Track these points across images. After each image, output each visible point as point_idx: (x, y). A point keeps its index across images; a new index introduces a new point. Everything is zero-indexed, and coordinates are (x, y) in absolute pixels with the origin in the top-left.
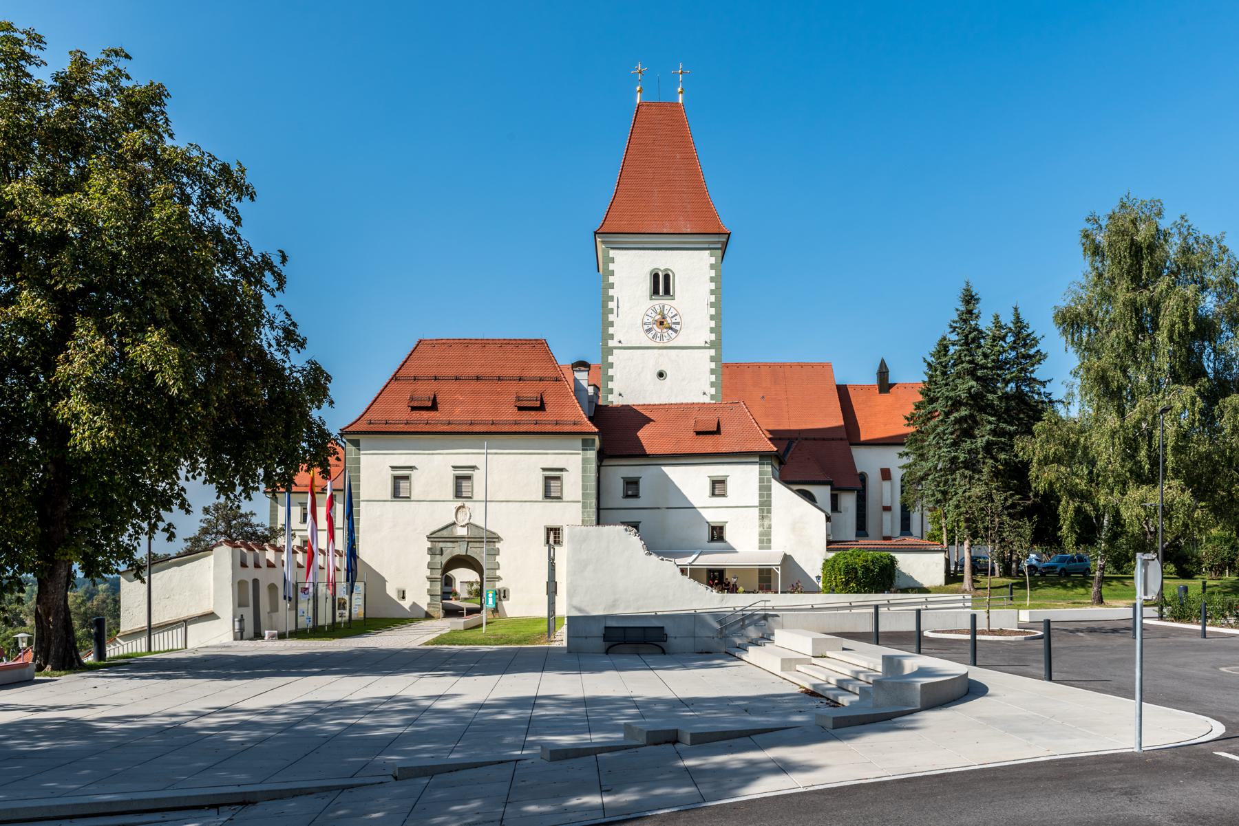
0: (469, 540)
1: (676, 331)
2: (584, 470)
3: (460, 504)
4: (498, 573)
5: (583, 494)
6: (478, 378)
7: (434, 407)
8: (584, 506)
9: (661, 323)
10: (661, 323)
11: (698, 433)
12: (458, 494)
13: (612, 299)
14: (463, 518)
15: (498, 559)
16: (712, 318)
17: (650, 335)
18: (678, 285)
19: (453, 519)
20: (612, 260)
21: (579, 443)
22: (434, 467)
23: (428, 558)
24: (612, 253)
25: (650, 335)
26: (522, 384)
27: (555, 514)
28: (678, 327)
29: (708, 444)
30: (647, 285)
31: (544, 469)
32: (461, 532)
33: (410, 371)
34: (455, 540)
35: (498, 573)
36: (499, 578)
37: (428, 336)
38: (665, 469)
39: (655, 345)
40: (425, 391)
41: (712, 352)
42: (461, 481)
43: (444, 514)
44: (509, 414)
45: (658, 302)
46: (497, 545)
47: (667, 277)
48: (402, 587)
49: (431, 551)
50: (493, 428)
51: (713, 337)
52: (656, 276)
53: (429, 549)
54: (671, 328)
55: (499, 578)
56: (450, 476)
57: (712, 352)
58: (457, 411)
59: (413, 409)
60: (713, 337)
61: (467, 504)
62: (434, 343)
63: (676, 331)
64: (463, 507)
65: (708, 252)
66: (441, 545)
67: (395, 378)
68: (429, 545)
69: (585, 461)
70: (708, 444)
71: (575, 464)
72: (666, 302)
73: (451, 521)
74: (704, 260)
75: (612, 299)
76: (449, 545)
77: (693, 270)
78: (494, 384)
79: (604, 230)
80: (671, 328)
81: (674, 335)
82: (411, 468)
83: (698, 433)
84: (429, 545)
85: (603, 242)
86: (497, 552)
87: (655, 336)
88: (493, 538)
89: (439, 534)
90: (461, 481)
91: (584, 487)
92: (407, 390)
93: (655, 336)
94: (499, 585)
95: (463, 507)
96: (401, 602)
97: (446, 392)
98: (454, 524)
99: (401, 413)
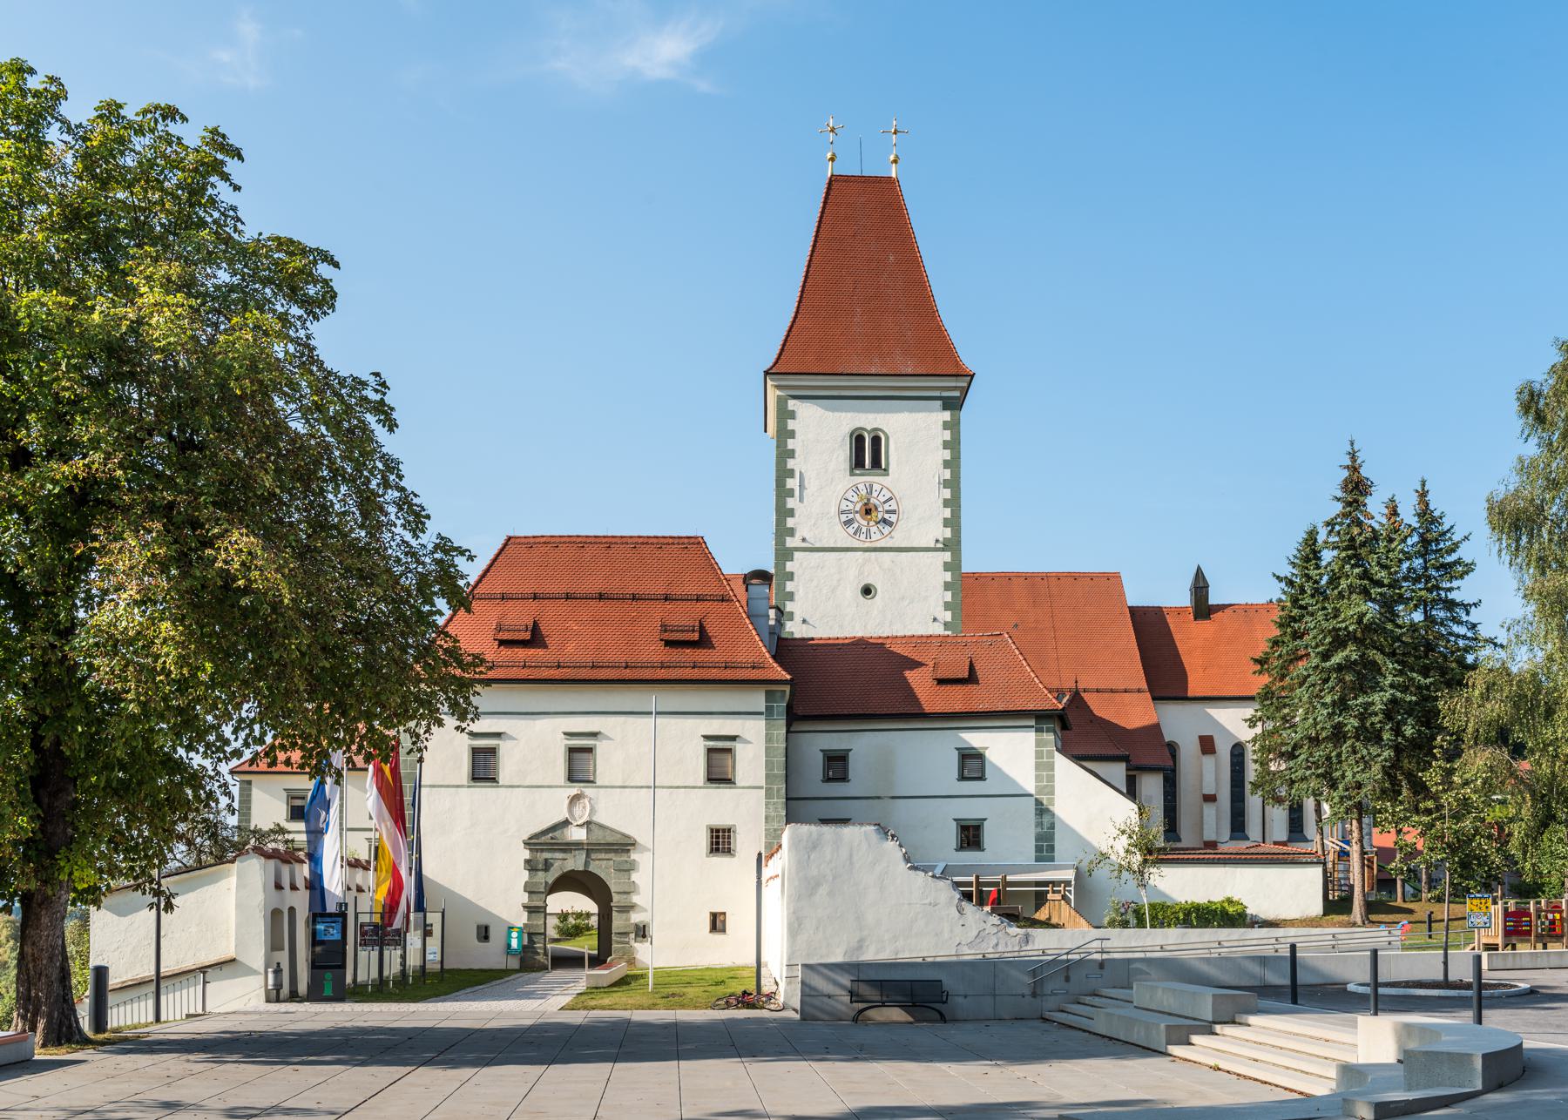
0: (590, 849)
1: (890, 524)
3: (574, 791)
4: (635, 899)
5: (767, 776)
6: (601, 597)
8: (769, 795)
11: (941, 682)
12: (572, 778)
13: (791, 473)
15: (635, 877)
17: (851, 530)
18: (894, 454)
20: (792, 415)
22: (533, 738)
23: (525, 876)
25: (851, 530)
26: (669, 606)
27: (722, 806)
28: (893, 518)
30: (844, 454)
32: (577, 834)
39: (857, 544)
43: (551, 807)
44: (653, 651)
45: (862, 480)
47: (876, 441)
49: (530, 865)
50: (628, 674)
52: (859, 440)
53: (527, 862)
58: (571, 647)
59: (502, 643)
61: (589, 791)
63: (890, 524)
68: (527, 854)
72: (877, 480)
75: (791, 473)
76: (558, 855)
78: (626, 606)
83: (941, 682)
84: (527, 854)
88: (623, 846)
89: (543, 839)
91: (769, 765)
94: (635, 918)
98: (566, 823)
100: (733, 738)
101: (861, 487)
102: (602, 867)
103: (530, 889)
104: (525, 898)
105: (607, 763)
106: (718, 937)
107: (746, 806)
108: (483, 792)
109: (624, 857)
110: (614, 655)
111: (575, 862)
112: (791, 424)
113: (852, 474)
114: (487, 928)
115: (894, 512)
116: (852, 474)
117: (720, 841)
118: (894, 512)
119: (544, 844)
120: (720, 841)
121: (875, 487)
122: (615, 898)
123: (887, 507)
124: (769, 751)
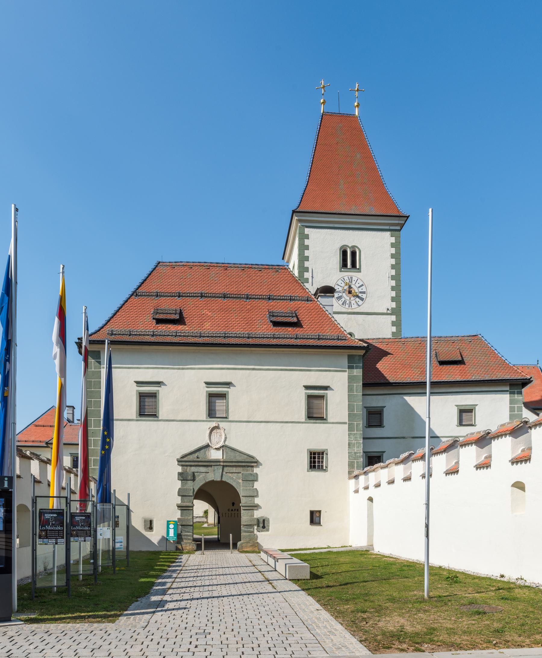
0: (225, 464)
1: (362, 299)
2: (350, 389)
3: (214, 424)
4: (257, 501)
5: (350, 415)
6: (225, 296)
7: (180, 321)
8: (351, 429)
9: (350, 292)
10: (350, 292)
11: (442, 363)
12: (211, 413)
13: (307, 270)
14: (218, 440)
15: (256, 485)
16: (393, 288)
18: (364, 260)
19: (206, 441)
20: (307, 237)
21: (345, 361)
22: (184, 383)
23: (178, 484)
24: (307, 231)
26: (272, 303)
27: (317, 436)
28: (364, 296)
29: (452, 374)
30: (337, 259)
31: (307, 387)
33: (153, 287)
34: (210, 464)
35: (257, 501)
36: (257, 507)
37: (167, 258)
38: (408, 398)
39: (344, 310)
40: (169, 305)
41: (393, 318)
42: (216, 399)
43: (196, 435)
44: (264, 329)
45: (346, 275)
46: (256, 470)
47: (354, 254)
48: (149, 516)
49: (182, 477)
50: (250, 341)
51: (394, 305)
52: (344, 253)
53: (180, 474)
54: (358, 296)
55: (257, 507)
56: (202, 392)
57: (393, 318)
58: (207, 325)
59: (159, 321)
60: (394, 305)
61: (222, 425)
62: (173, 266)
63: (362, 299)
64: (217, 427)
65: (388, 233)
66: (193, 469)
67: (135, 293)
68: (180, 469)
69: (351, 379)
70: (452, 374)
71: (340, 383)
72: (354, 275)
73: (204, 443)
74: (385, 239)
75: (307, 270)
76: (202, 469)
77: (375, 247)
78: (243, 302)
79: (297, 210)
80: (358, 296)
81: (360, 302)
82: (159, 383)
83: (442, 363)
84: (180, 469)
85: (299, 221)
86: (255, 478)
87: (344, 303)
88: (248, 463)
89: (191, 458)
90: (216, 399)
91: (351, 408)
92: (150, 304)
93: (344, 303)
94: (257, 514)
95: (217, 427)
96: (148, 534)
97: (190, 308)
98: (208, 446)
99: (145, 325)
100: (326, 388)
101: (346, 278)
102: (234, 478)
103: (182, 493)
104: (179, 500)
105: (238, 403)
106: (316, 528)
107: (337, 436)
108: (147, 425)
109: (249, 471)
110: (239, 330)
111: (214, 475)
112: (307, 242)
113: (341, 271)
114: (151, 522)
115: (364, 293)
116: (341, 271)
117: (316, 460)
118: (364, 293)
119: (192, 461)
120: (316, 460)
121: (354, 279)
122: (243, 501)
123: (360, 290)
124: (351, 398)
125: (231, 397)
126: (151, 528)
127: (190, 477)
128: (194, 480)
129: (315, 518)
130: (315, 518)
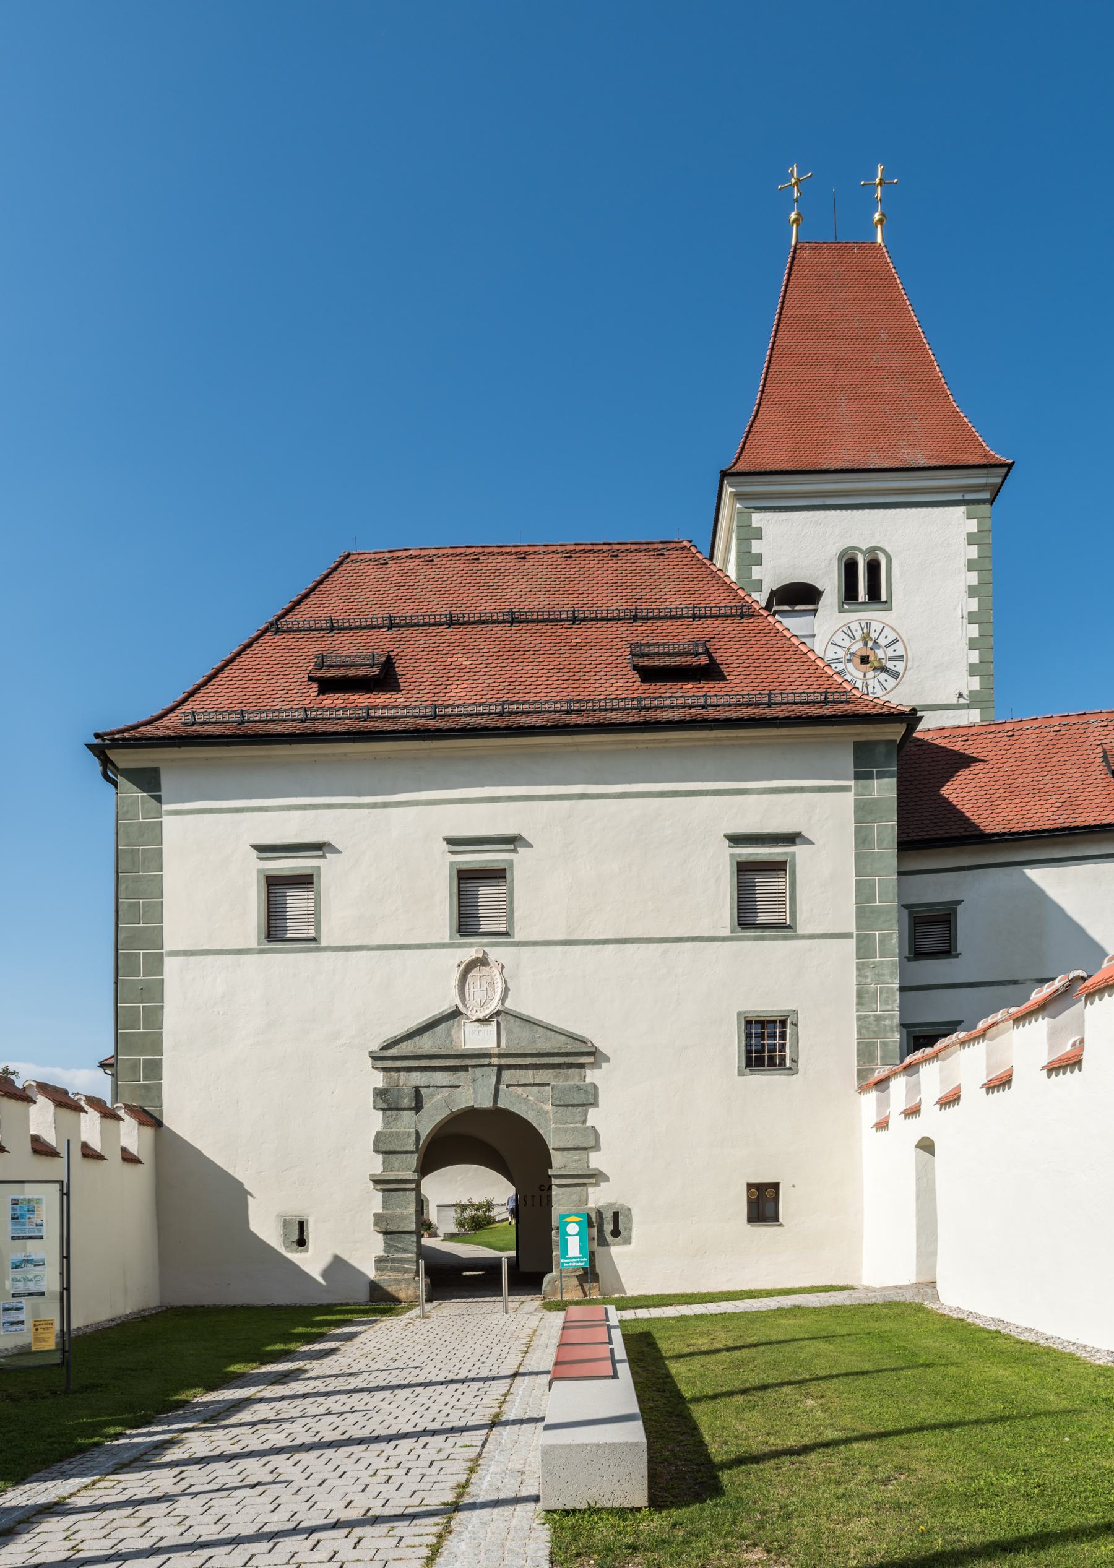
0: (504, 1064)
2: (862, 839)
3: (472, 953)
4: (596, 1160)
5: (860, 913)
8: (864, 950)
12: (466, 923)
15: (594, 1117)
22: (384, 843)
23: (376, 1121)
31: (736, 840)
34: (460, 1062)
35: (596, 1160)
36: (597, 1177)
42: (476, 887)
43: (424, 984)
46: (592, 1076)
48: (296, 1209)
53: (379, 1093)
55: (597, 1177)
61: (494, 954)
64: (482, 962)
68: (379, 1080)
69: (864, 810)
71: (832, 822)
73: (445, 1007)
84: (379, 1080)
86: (590, 1098)
90: (476, 887)
91: (863, 891)
94: (598, 1197)
96: (295, 1257)
98: (455, 1014)
100: (790, 839)
102: (531, 1101)
103: (384, 1147)
104: (376, 1165)
105: (537, 894)
106: (764, 1231)
109: (572, 1078)
111: (474, 1093)
114: (301, 1225)
117: (765, 1044)
119: (407, 1059)
120: (765, 1044)
122: (559, 1162)
125: (518, 876)
126: (302, 1242)
127: (406, 1102)
128: (418, 1107)
129: (763, 1204)
130: (763, 1204)
